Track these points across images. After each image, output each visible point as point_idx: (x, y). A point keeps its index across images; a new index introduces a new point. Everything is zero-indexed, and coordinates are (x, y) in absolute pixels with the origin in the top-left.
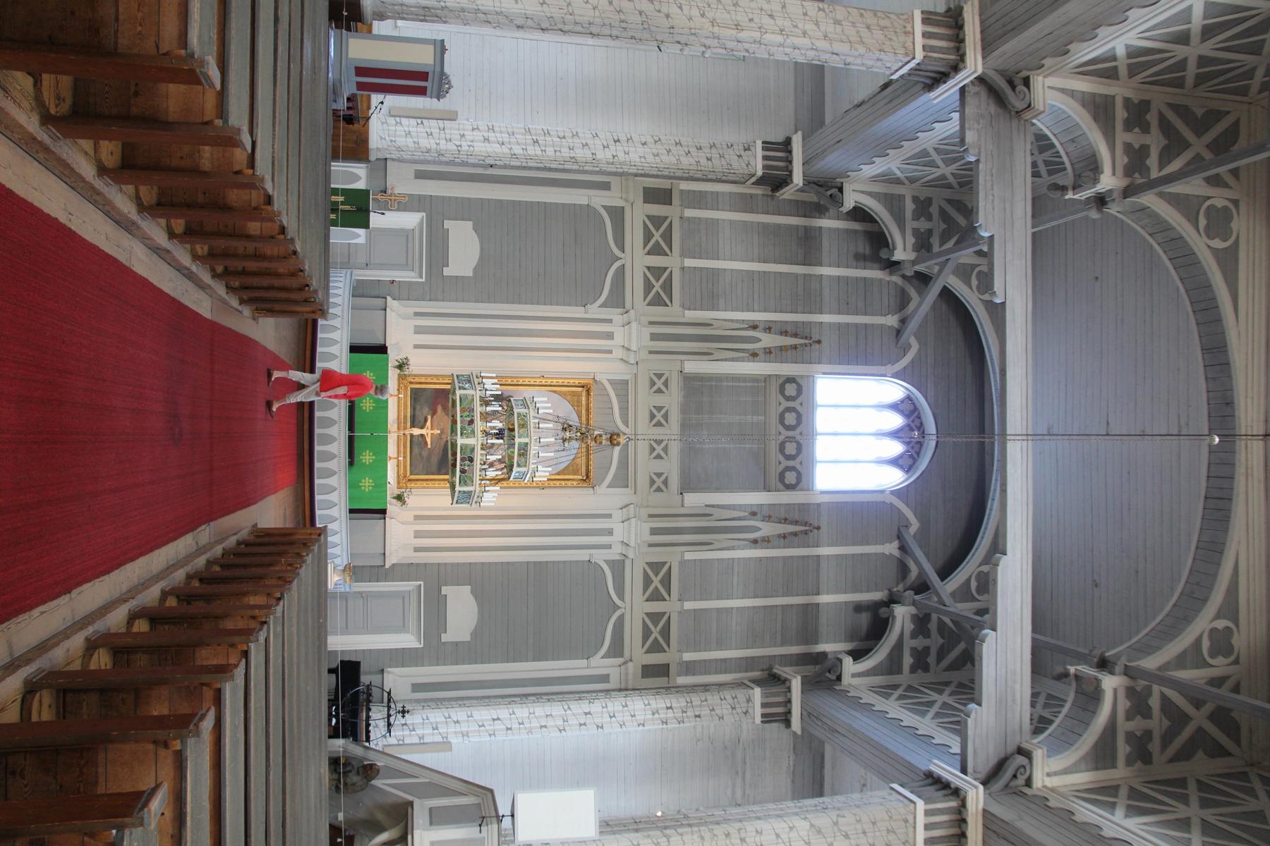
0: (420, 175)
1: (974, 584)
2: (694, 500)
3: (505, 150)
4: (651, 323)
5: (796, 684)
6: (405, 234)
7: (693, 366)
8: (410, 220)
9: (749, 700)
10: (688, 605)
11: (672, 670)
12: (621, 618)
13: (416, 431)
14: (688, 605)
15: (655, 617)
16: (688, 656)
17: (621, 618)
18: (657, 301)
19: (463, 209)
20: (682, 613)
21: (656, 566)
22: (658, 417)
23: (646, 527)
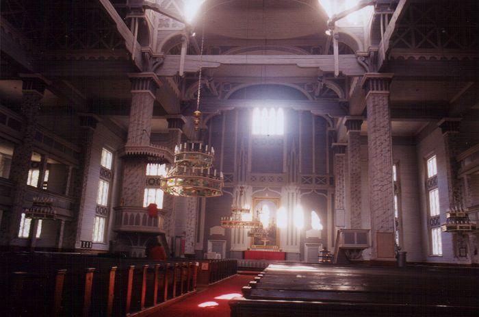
0: (198, 241)
1: (310, 91)
2: (285, 170)
3: (194, 219)
4: (237, 180)
5: (334, 144)
6: (213, 245)
7: (249, 169)
8: (210, 245)
9: (338, 157)
10: (314, 171)
11: (331, 176)
12: (317, 190)
13: (265, 244)
14: (314, 171)
15: (317, 181)
16: (328, 172)
17: (317, 190)
18: (232, 178)
19: (207, 230)
20: (317, 173)
21: (303, 180)
22: (263, 180)
23: (292, 183)
